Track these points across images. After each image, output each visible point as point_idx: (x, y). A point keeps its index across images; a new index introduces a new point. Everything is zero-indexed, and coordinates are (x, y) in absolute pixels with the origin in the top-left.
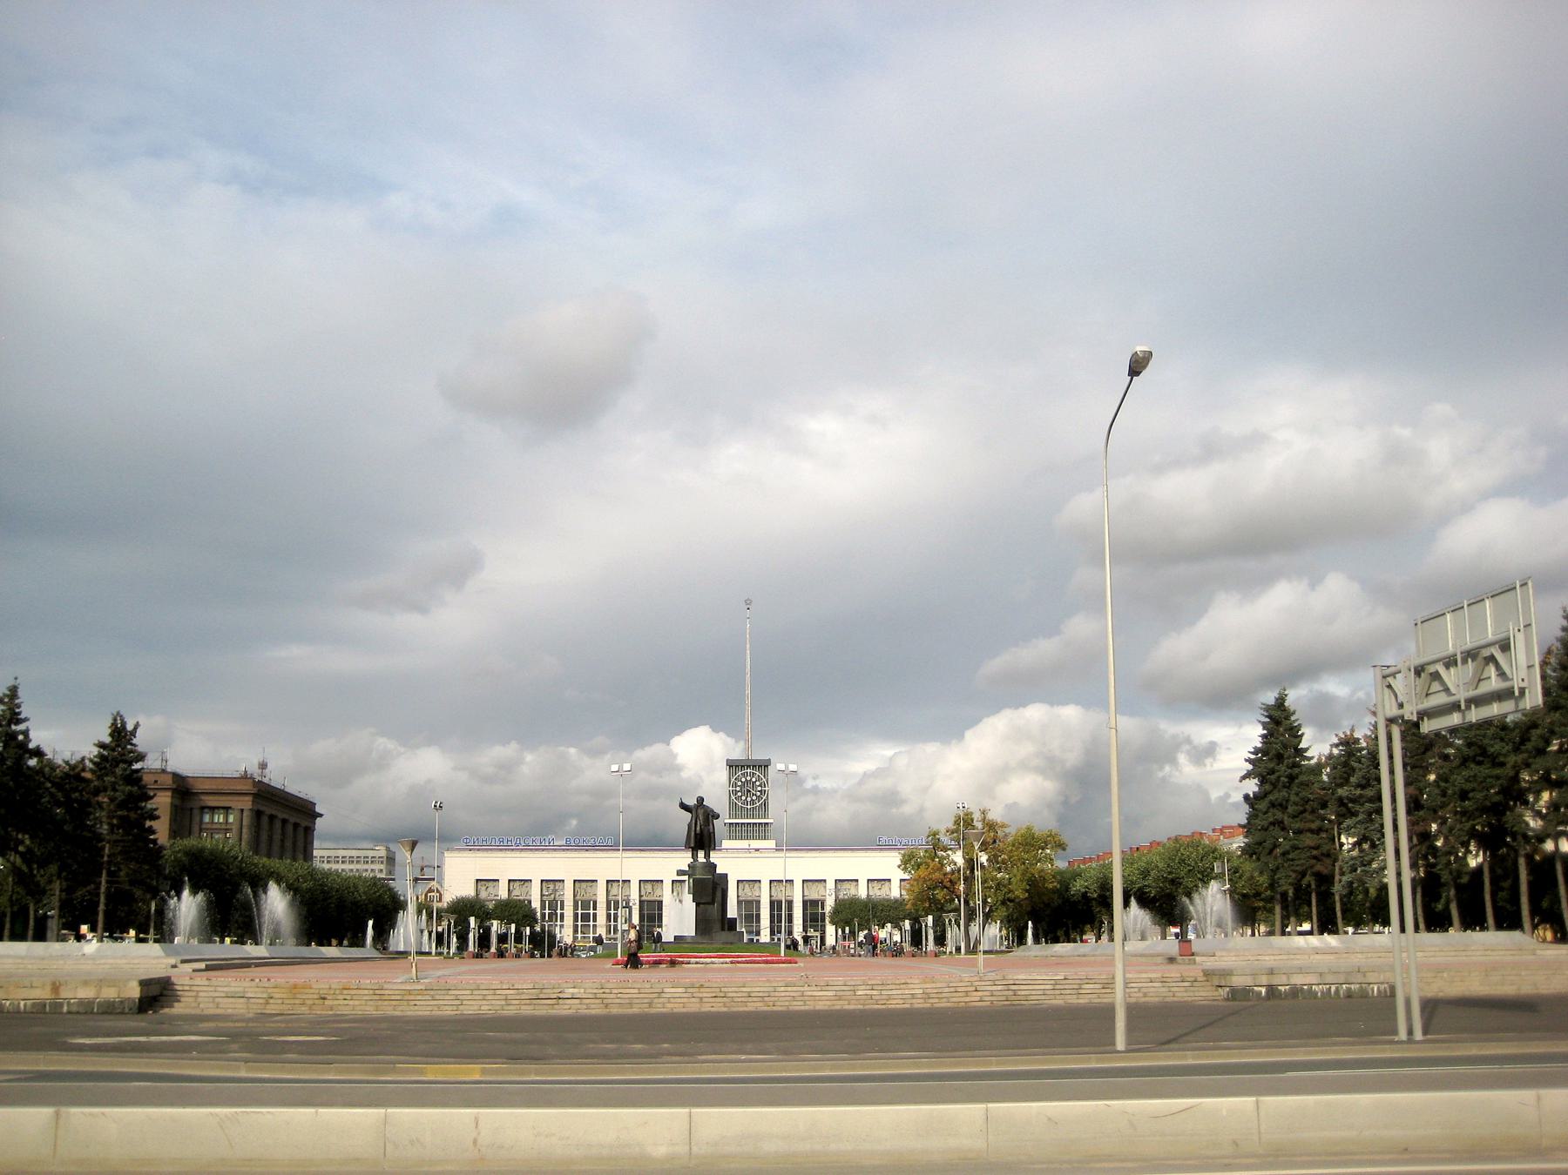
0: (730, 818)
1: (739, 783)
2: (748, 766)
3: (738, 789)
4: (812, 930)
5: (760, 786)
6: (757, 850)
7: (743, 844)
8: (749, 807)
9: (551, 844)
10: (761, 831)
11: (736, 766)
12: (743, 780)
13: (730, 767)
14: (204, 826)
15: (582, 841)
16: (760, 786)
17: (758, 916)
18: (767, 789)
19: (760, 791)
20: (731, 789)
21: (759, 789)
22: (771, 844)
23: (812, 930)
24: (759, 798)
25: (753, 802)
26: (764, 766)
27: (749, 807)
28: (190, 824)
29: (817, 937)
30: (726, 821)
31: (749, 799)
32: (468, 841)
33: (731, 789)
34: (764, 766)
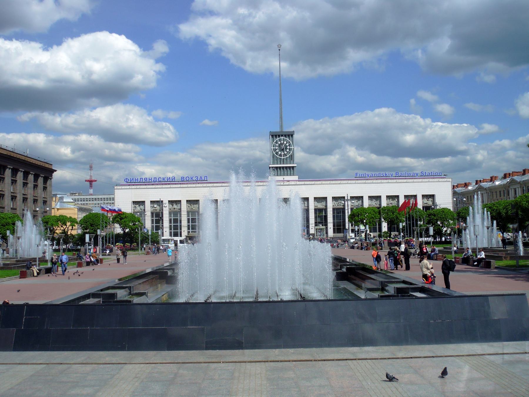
2: (282, 136)
3: (277, 148)
4: (321, 225)
5: (289, 145)
6: (289, 181)
8: (283, 158)
9: (173, 180)
10: (290, 170)
11: (275, 135)
12: (279, 143)
13: (272, 136)
15: (190, 178)
16: (289, 145)
19: (290, 149)
20: (273, 148)
22: (296, 178)
23: (321, 225)
26: (290, 135)
29: (324, 229)
30: (270, 166)
32: (128, 180)
33: (273, 148)
34: (290, 135)
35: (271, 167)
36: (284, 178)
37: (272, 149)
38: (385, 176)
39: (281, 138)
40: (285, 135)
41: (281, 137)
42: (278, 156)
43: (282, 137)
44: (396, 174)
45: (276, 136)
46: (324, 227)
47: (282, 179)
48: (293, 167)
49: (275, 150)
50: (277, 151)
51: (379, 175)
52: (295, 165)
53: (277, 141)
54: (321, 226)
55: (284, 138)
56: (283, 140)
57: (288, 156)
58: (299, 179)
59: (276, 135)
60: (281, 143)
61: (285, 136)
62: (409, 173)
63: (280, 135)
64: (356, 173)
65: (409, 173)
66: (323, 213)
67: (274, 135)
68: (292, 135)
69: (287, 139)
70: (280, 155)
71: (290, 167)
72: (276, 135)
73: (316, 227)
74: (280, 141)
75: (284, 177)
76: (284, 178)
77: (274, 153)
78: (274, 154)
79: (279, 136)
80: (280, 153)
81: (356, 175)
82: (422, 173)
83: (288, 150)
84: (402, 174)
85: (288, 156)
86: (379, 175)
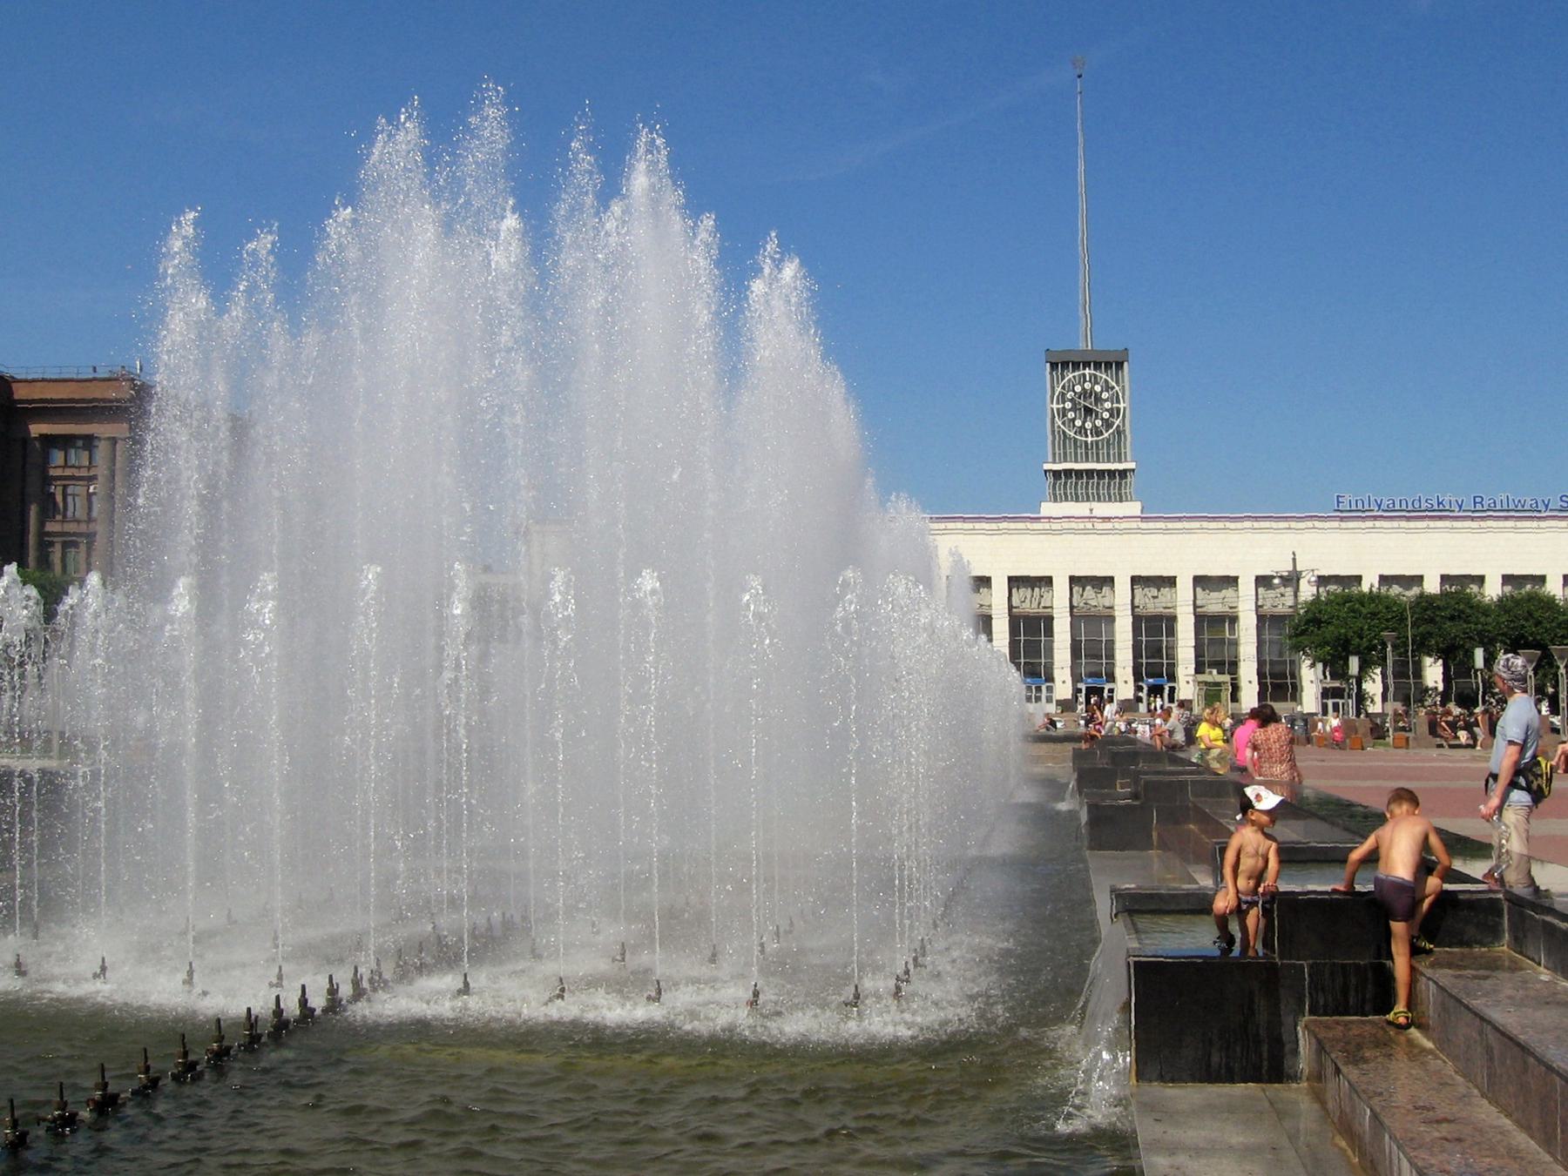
0: (1054, 462)
1: (1070, 395)
2: (1087, 364)
4: (1215, 671)
7: (1081, 508)
8: (1090, 439)
11: (1063, 364)
12: (1078, 389)
13: (1054, 366)
14: (52, 472)
17: (1111, 644)
18: (1122, 406)
19: (1111, 411)
20: (1055, 406)
21: (1108, 405)
22: (1134, 508)
23: (1215, 671)
24: (1108, 424)
25: (1098, 433)
27: (1090, 439)
28: (24, 466)
30: (1047, 466)
31: (1088, 425)
33: (1055, 406)
35: (1050, 471)
36: (1091, 510)
37: (1052, 409)
38: (1436, 507)
39: (1082, 372)
40: (1095, 363)
41: (1084, 369)
42: (1072, 434)
43: (1087, 371)
44: (1475, 503)
45: (1065, 365)
46: (1226, 678)
47: (1087, 514)
48: (1123, 474)
49: (1064, 412)
50: (1071, 415)
51: (1417, 506)
52: (1132, 465)
53: (1069, 380)
54: (1213, 676)
55: (1093, 372)
56: (1090, 381)
57: (1106, 435)
58: (1142, 512)
59: (1068, 363)
60: (1083, 389)
61: (1097, 366)
62: (1519, 501)
63: (1079, 363)
64: (1338, 497)
65: (1519, 501)
66: (1224, 631)
67: (1061, 364)
68: (1120, 365)
69: (1104, 376)
70: (1082, 430)
71: (1112, 473)
72: (1068, 363)
73: (1201, 678)
74: (1079, 383)
75: (1095, 505)
76: (1091, 510)
77: (1060, 423)
78: (1059, 427)
79: (1076, 366)
80: (1078, 423)
81: (1338, 502)
82: (1564, 498)
83: (1106, 415)
84: (1495, 503)
85: (1106, 435)
86: (1417, 506)
